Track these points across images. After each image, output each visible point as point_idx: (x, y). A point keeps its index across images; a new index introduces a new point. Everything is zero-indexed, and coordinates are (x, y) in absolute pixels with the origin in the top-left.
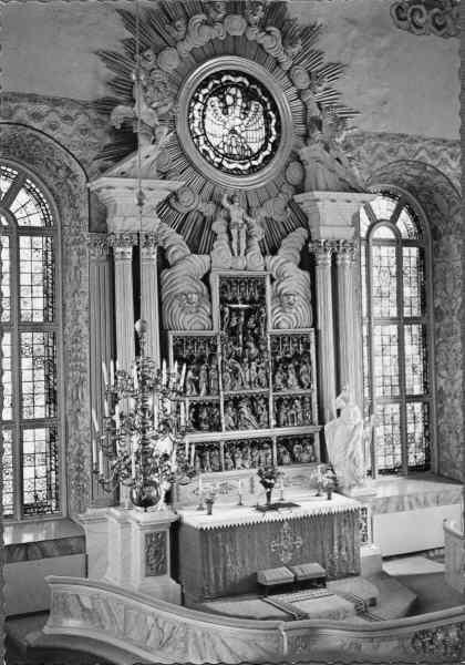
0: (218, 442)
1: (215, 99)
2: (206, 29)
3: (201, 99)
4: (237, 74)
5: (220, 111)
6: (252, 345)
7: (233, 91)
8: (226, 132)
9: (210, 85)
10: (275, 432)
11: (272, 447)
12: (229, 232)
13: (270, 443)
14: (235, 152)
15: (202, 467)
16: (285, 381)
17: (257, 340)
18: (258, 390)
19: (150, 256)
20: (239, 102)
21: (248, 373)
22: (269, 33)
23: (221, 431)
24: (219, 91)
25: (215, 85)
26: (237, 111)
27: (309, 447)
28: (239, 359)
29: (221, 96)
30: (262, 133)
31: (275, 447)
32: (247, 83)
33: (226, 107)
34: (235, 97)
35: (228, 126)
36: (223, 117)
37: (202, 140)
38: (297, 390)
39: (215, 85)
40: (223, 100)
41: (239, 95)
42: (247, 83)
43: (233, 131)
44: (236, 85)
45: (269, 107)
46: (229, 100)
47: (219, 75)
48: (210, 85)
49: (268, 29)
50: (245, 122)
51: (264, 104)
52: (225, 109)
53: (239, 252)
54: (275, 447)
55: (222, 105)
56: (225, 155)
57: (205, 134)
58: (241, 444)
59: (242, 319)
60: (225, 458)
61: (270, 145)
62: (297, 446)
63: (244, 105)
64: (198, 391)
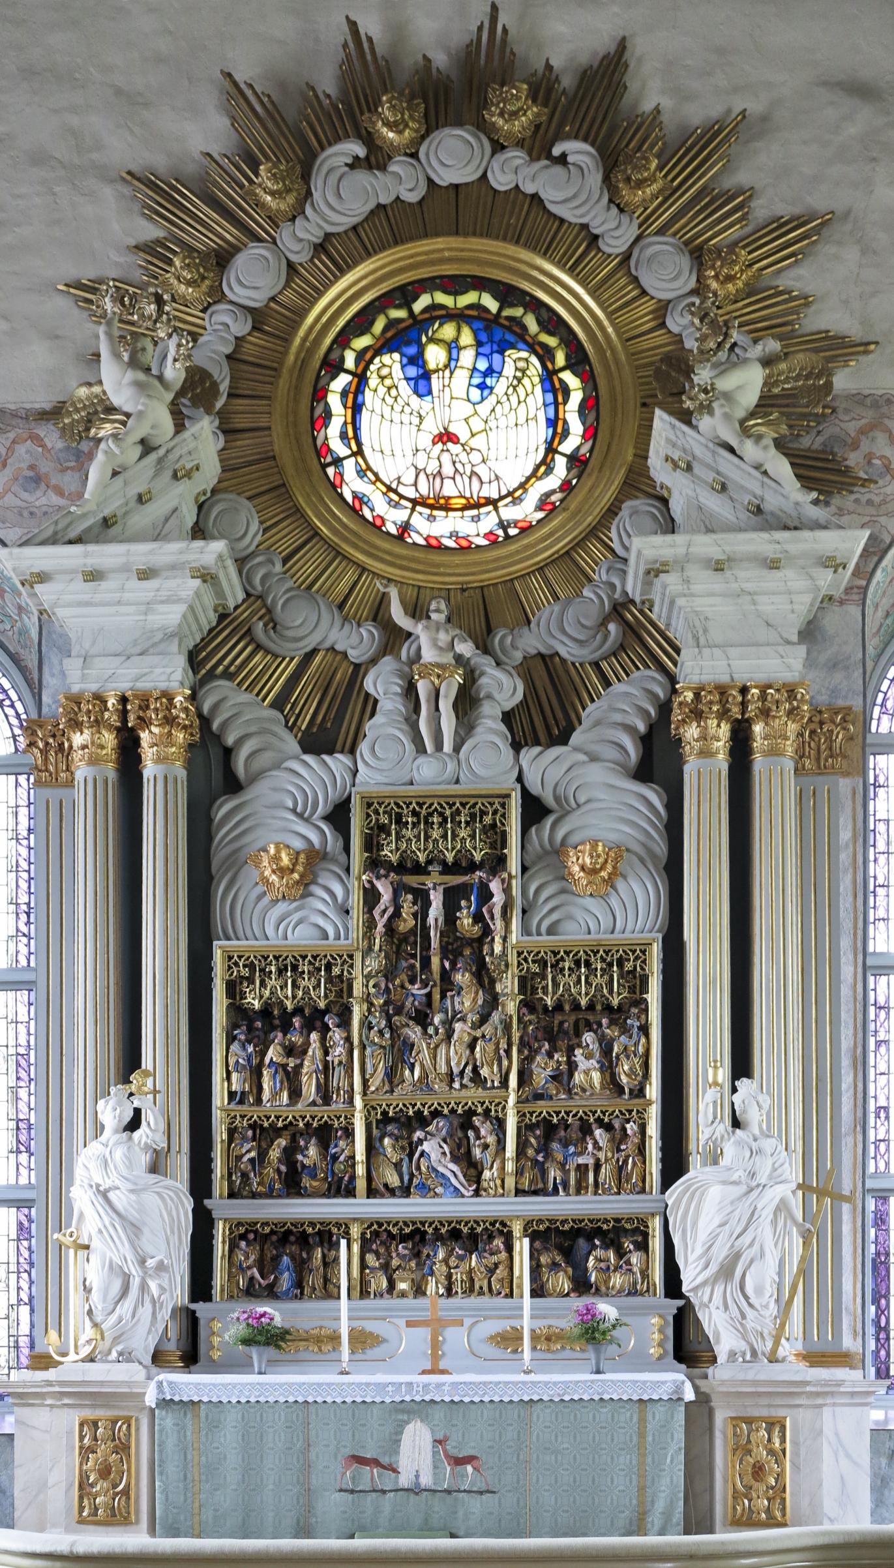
1: (392, 361)
2: (362, 177)
3: (350, 361)
4: (454, 285)
5: (405, 389)
6: (462, 978)
7: (448, 331)
8: (425, 440)
9: (379, 326)
10: (518, 1209)
11: (509, 1248)
12: (410, 690)
14: (449, 489)
18: (473, 1095)
19: (161, 764)
20: (467, 357)
22: (562, 160)
23: (351, 1193)
24: (406, 339)
25: (391, 324)
26: (461, 376)
27: (635, 1258)
28: (422, 1019)
29: (412, 350)
30: (542, 432)
32: (491, 304)
33: (426, 375)
34: (453, 347)
35: (433, 426)
36: (415, 401)
37: (349, 466)
38: (603, 1103)
39: (391, 324)
40: (417, 360)
41: (467, 338)
42: (491, 304)
43: (446, 437)
44: (458, 317)
45: (560, 359)
46: (435, 355)
47: (405, 295)
48: (379, 326)
49: (556, 151)
50: (484, 409)
51: (545, 355)
52: (422, 382)
53: (439, 746)
55: (412, 371)
56: (415, 502)
57: (360, 452)
58: (417, 1237)
60: (363, 1265)
61: (561, 463)
63: (482, 365)
64: (295, 1094)
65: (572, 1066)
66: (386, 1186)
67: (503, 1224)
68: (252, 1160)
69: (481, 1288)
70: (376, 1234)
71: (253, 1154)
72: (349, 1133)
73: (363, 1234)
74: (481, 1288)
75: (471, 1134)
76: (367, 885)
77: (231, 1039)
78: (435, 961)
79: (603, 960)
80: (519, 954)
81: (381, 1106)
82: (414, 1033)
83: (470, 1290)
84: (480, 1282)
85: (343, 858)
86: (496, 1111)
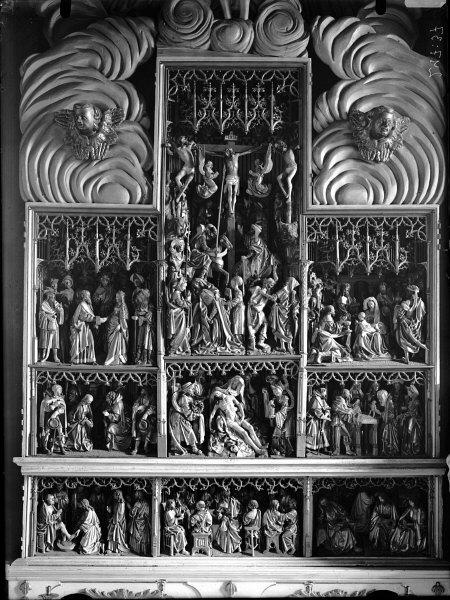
0: (148, 482)
13: (299, 497)
15: (104, 538)
16: (351, 343)
17: (278, 242)
21: (240, 317)
28: (218, 279)
31: (309, 506)
54: (309, 506)
58: (212, 490)
59: (234, 180)
62: (384, 509)
64: (102, 351)
65: (356, 332)
66: (183, 444)
67: (295, 484)
68: (61, 416)
69: (273, 545)
70: (175, 490)
71: (61, 411)
72: (153, 392)
73: (164, 490)
74: (273, 545)
75: (265, 392)
76: (171, 152)
77: (41, 297)
78: (231, 224)
79: (386, 228)
80: (310, 221)
81: (182, 366)
82: (213, 294)
83: (261, 549)
84: (272, 538)
85: (145, 120)
86: (288, 372)
